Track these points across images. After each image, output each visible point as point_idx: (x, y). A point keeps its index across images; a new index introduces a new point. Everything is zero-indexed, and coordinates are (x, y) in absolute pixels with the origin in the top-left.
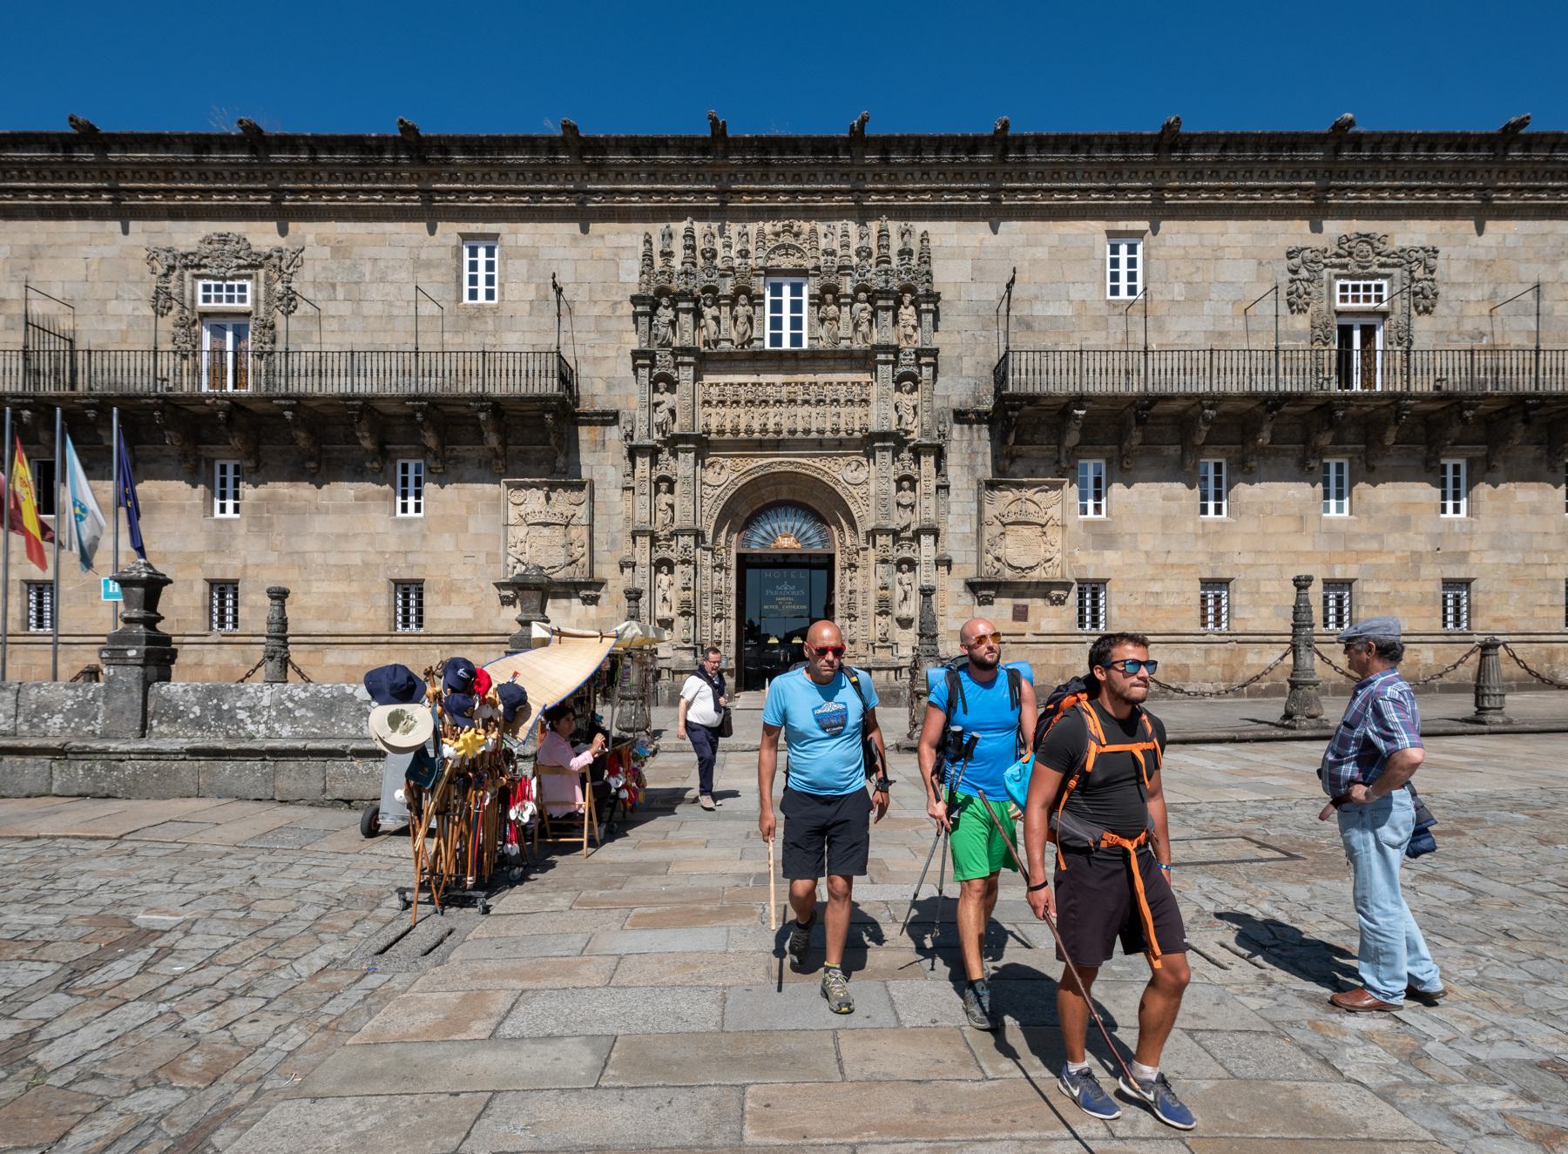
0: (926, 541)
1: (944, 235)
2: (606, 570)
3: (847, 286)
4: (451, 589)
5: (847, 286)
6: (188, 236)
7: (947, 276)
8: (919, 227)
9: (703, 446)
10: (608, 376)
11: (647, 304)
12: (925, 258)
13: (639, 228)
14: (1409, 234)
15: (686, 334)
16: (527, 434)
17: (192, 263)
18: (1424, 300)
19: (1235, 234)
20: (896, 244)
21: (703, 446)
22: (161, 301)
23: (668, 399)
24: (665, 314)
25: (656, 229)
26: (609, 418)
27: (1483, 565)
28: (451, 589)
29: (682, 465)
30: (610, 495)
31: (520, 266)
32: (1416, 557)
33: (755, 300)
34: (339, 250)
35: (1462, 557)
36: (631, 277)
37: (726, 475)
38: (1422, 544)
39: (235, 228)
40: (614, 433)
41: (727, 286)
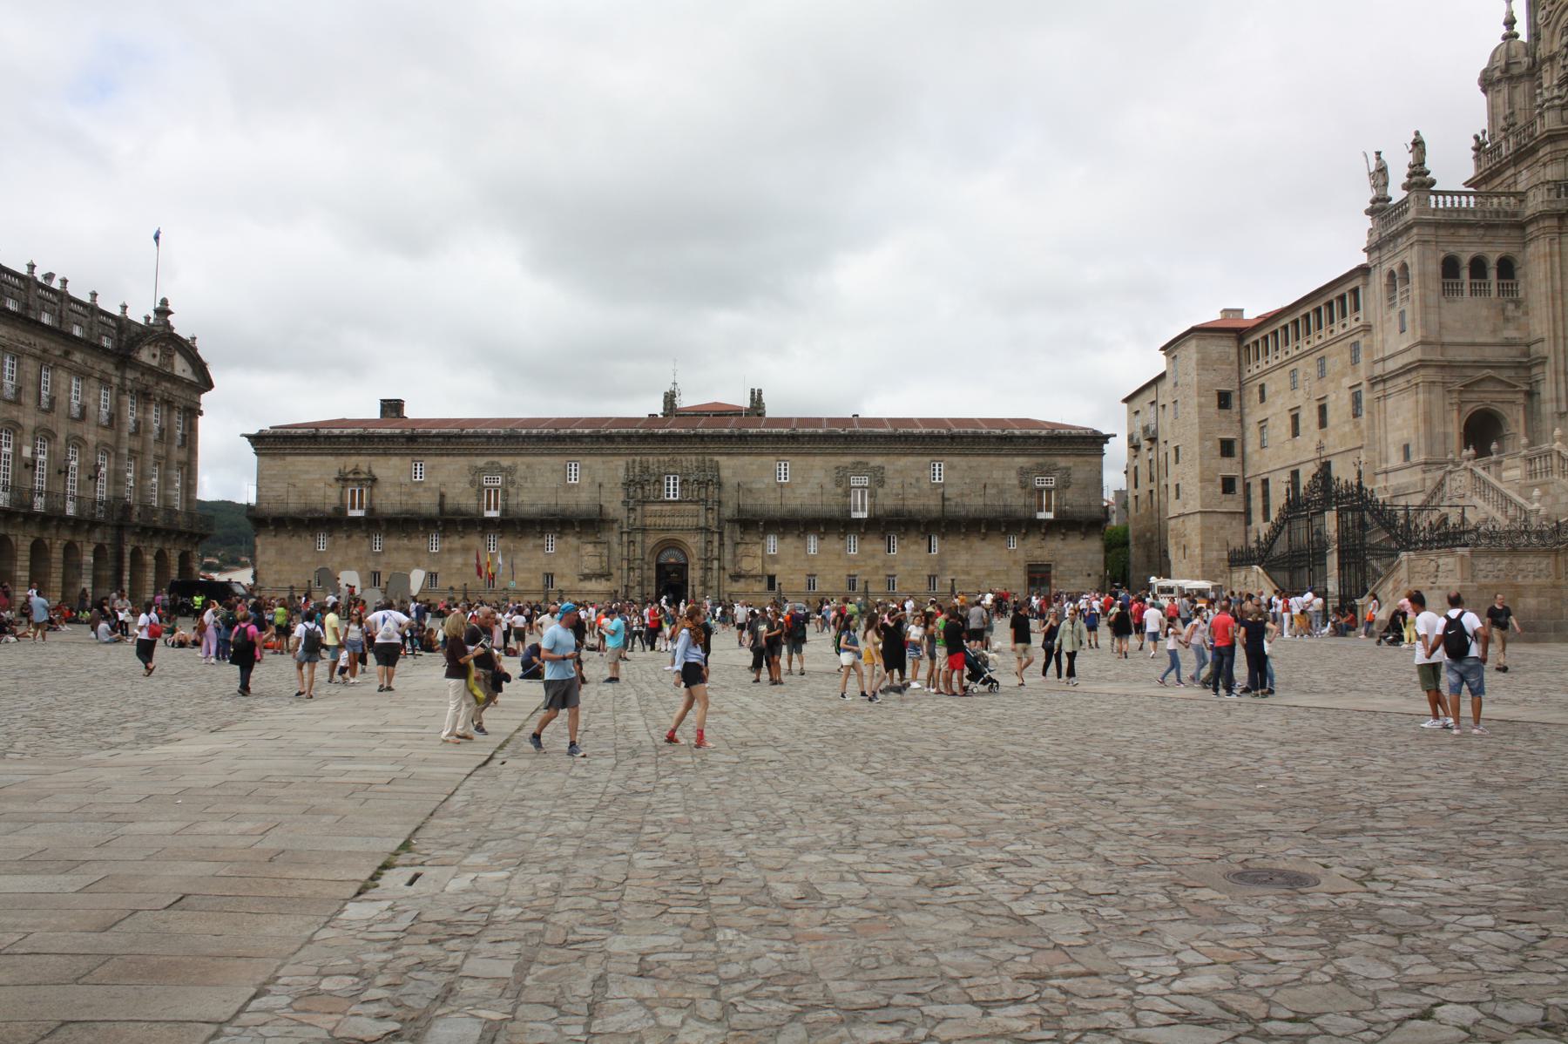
1: (723, 460)
2: (613, 571)
4: (563, 576)
6: (481, 462)
7: (725, 474)
8: (716, 458)
9: (644, 530)
10: (614, 505)
11: (628, 484)
14: (876, 461)
16: (588, 524)
17: (481, 470)
18: (881, 483)
19: (818, 461)
21: (644, 530)
22: (472, 483)
25: (630, 459)
26: (614, 521)
27: (900, 570)
28: (563, 576)
31: (586, 471)
33: (661, 483)
34: (529, 466)
35: (892, 567)
36: (621, 473)
37: (652, 540)
38: (879, 563)
39: (496, 459)
40: (616, 526)
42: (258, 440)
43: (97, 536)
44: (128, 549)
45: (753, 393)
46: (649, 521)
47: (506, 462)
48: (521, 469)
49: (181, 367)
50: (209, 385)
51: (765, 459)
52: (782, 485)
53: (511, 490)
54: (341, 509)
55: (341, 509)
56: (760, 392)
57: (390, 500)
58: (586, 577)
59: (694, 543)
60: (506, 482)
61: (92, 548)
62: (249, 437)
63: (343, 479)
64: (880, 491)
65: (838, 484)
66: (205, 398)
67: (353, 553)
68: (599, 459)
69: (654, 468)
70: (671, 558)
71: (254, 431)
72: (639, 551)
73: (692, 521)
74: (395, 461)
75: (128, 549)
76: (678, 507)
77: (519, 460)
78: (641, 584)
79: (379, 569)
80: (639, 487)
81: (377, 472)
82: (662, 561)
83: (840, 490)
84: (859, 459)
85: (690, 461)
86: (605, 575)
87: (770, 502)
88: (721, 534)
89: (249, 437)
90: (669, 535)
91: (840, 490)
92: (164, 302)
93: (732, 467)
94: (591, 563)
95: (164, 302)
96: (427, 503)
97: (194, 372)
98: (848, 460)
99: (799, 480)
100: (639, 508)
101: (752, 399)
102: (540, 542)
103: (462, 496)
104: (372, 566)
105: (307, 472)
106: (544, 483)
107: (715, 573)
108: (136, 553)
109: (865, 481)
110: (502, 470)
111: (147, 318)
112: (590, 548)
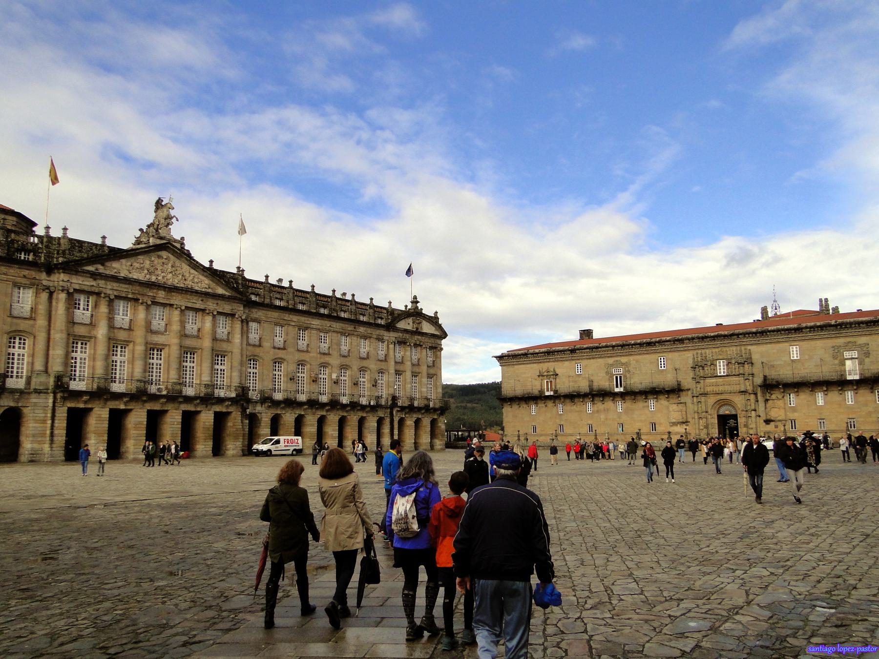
0: (753, 412)
3: (733, 362)
5: (733, 362)
6: (611, 361)
7: (755, 357)
8: (749, 347)
9: (705, 394)
10: (687, 381)
11: (694, 368)
12: (750, 354)
13: (691, 352)
14: (863, 340)
15: (702, 373)
17: (612, 365)
18: (867, 354)
20: (744, 352)
21: (705, 394)
22: (607, 373)
23: (699, 386)
24: (697, 370)
25: (695, 352)
26: (688, 390)
29: (703, 399)
30: (689, 405)
32: (870, 412)
34: (637, 361)
36: (691, 361)
37: (711, 400)
39: (618, 358)
40: (690, 392)
41: (709, 363)
42: (500, 358)
43: (381, 414)
44: (396, 420)
45: (821, 300)
46: (709, 389)
47: (624, 360)
48: (633, 363)
49: (427, 328)
50: (444, 335)
51: (781, 345)
52: (792, 361)
53: (628, 376)
54: (541, 392)
55: (541, 392)
56: (826, 300)
57: (564, 385)
58: (674, 424)
59: (739, 401)
60: (625, 371)
61: (376, 419)
62: (496, 357)
63: (541, 375)
64: (867, 360)
65: (834, 358)
66: (444, 342)
67: (549, 415)
68: (676, 354)
69: (709, 357)
70: (726, 411)
71: (499, 354)
72: (704, 408)
73: (737, 388)
74: (567, 363)
75: (396, 420)
76: (727, 379)
77: (631, 358)
78: (707, 427)
79: (562, 423)
80: (701, 368)
81: (558, 371)
82: (721, 413)
83: (837, 362)
84: (849, 339)
85: (732, 350)
86: (686, 422)
87: (786, 374)
88: (756, 394)
89: (496, 357)
90: (722, 397)
91: (837, 362)
92: (415, 297)
93: (759, 351)
94: (676, 416)
95: (415, 297)
96: (584, 387)
97: (436, 330)
98: (841, 341)
99: (807, 357)
100: (702, 381)
101: (821, 305)
102: (646, 404)
103: (602, 382)
104: (558, 422)
105: (525, 373)
106: (645, 370)
107: (753, 419)
108: (401, 422)
109: (855, 354)
110: (623, 364)
111: (406, 306)
112: (675, 407)
